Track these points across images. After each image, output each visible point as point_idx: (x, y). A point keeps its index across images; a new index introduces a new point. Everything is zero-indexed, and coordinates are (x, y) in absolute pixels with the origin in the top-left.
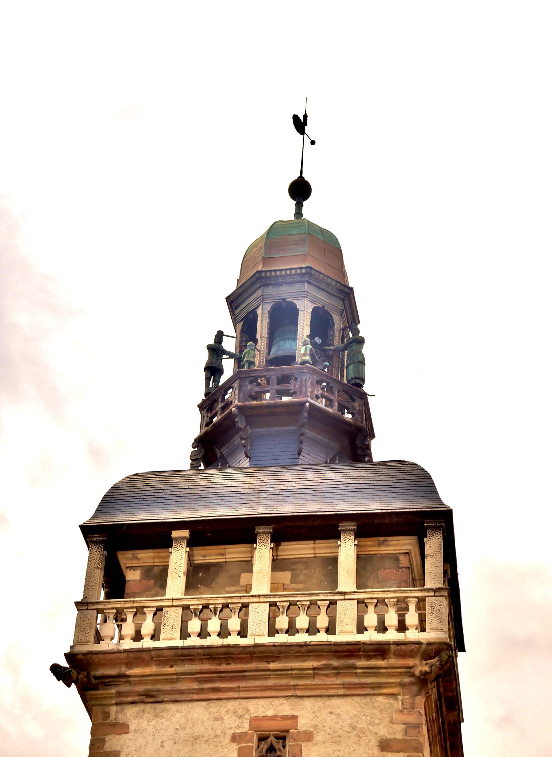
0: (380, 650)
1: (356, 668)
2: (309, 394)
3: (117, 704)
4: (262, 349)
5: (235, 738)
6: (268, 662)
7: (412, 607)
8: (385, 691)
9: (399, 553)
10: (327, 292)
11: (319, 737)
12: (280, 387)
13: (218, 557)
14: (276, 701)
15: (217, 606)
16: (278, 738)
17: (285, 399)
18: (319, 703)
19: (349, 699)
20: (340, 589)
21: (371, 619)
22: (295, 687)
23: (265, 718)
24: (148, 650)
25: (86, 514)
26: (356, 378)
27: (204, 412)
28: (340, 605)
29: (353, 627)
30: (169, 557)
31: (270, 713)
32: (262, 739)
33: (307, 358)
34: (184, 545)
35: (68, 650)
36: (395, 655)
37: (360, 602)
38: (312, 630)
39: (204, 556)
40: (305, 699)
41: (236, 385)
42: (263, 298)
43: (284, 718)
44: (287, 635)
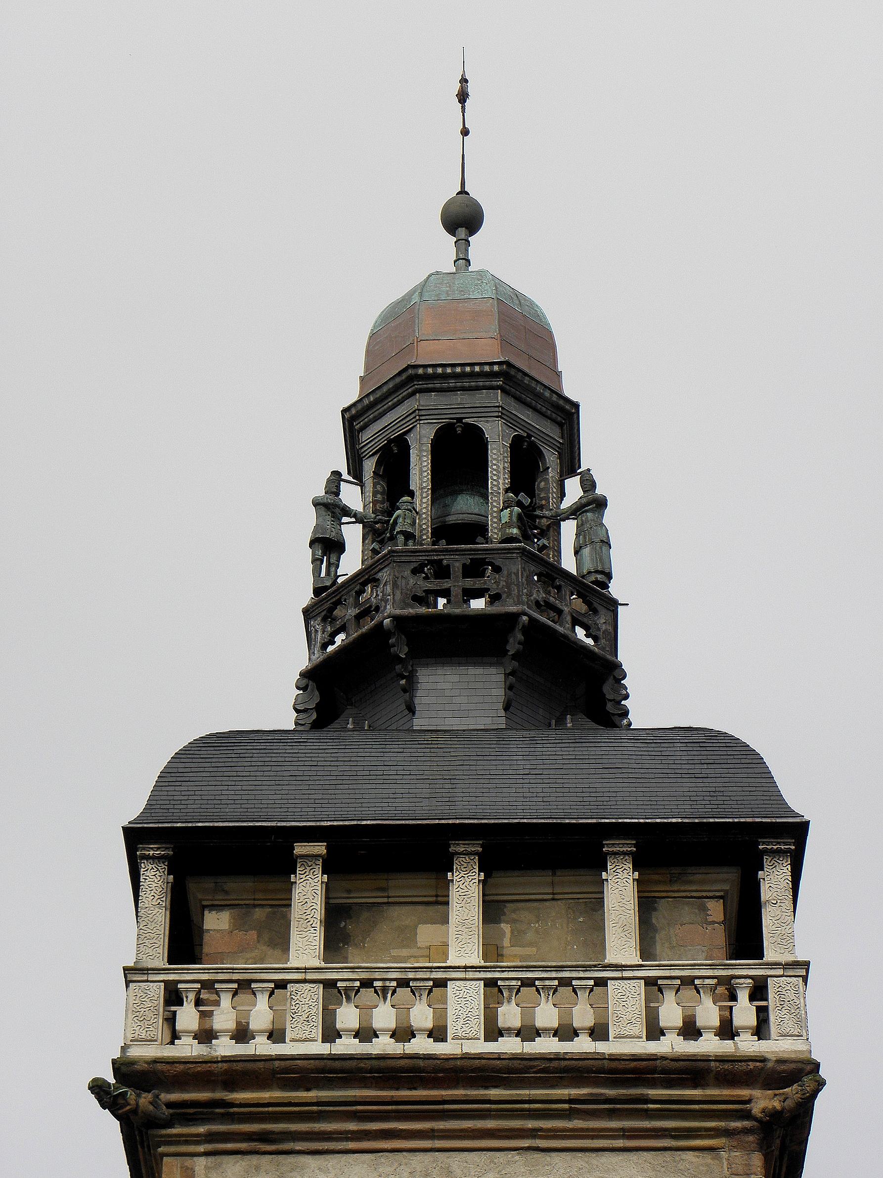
0: (692, 1071)
2: (525, 598)
4: (424, 511)
6: (486, 1088)
7: (743, 996)
9: (707, 897)
10: (535, 410)
12: (469, 583)
13: (374, 894)
15: (387, 983)
17: (478, 604)
18: (579, 1161)
19: (634, 1157)
20: (610, 959)
25: (132, 807)
26: (597, 572)
27: (316, 624)
29: (640, 1028)
30: (290, 891)
33: (515, 531)
34: (318, 870)
35: (117, 1055)
36: (717, 1079)
37: (650, 982)
38: (566, 1032)
39: (349, 891)
40: (553, 1154)
41: (384, 575)
42: (418, 415)
44: (519, 1039)
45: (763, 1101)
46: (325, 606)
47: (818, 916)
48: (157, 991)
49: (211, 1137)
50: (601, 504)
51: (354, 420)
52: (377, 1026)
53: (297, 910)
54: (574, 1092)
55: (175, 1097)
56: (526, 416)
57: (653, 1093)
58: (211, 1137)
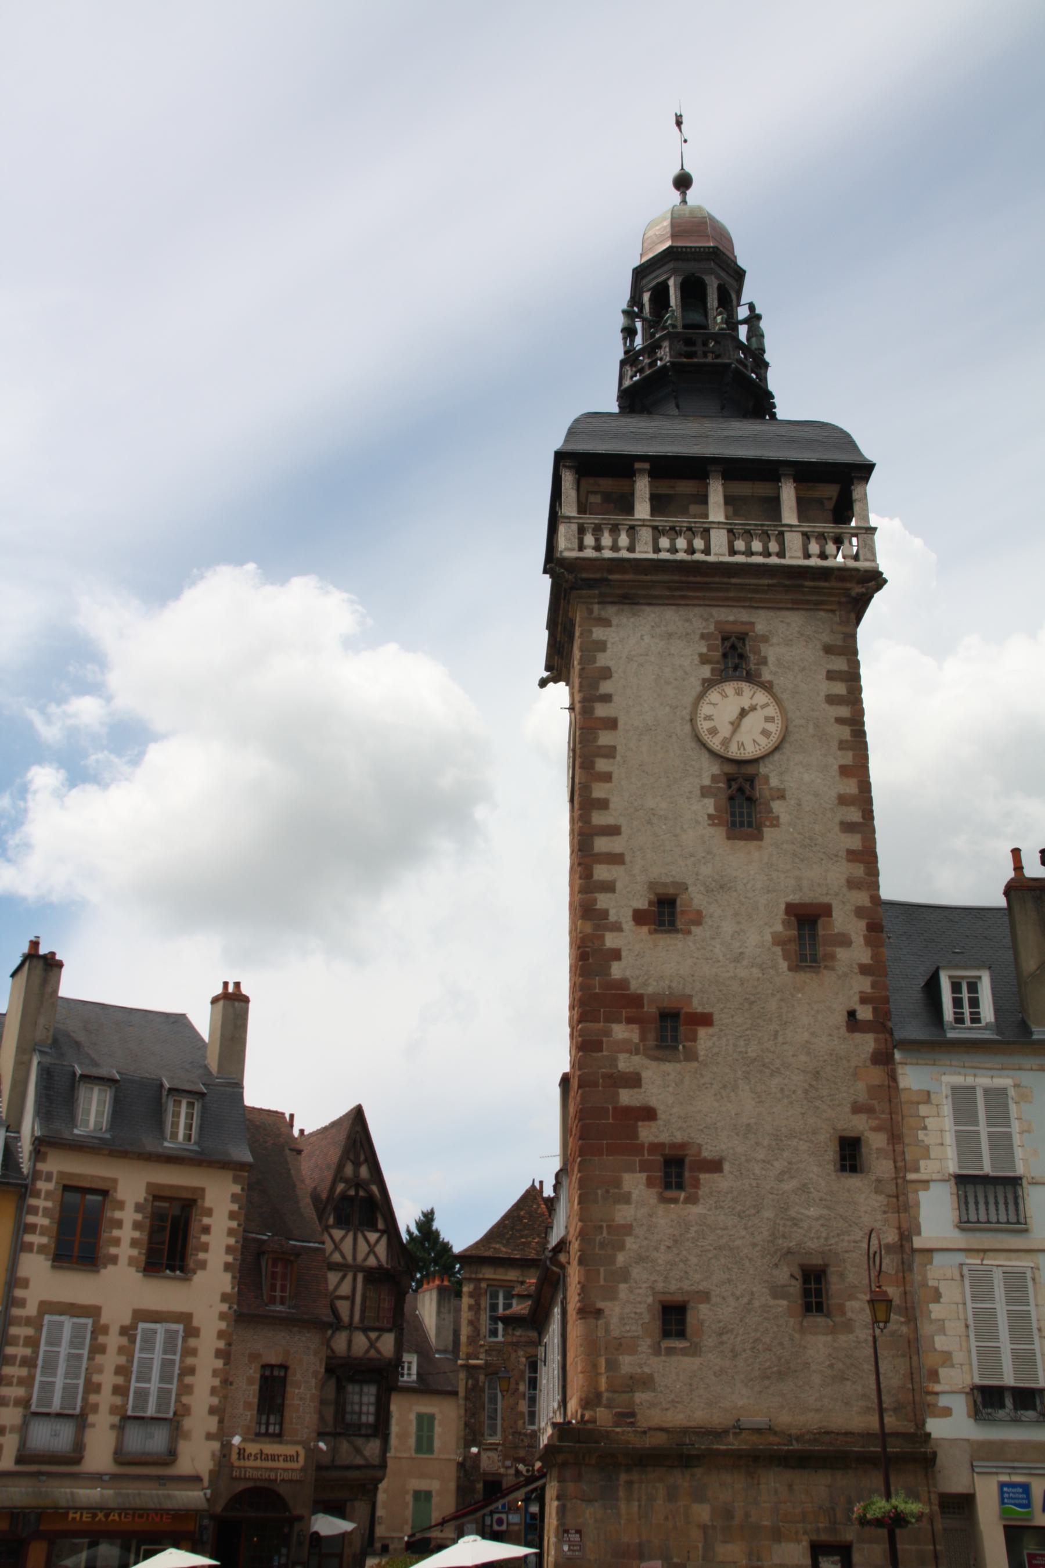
1: (803, 586)
3: (599, 603)
5: (703, 637)
8: (825, 607)
11: (774, 640)
14: (735, 610)
16: (738, 638)
18: (771, 613)
21: (814, 548)
23: (727, 622)
24: (629, 560)
28: (787, 535)
29: (800, 554)
31: (731, 618)
32: (724, 639)
33: (724, 326)
34: (646, 476)
38: (767, 554)
43: (743, 623)
46: (630, 359)
47: (881, 505)
48: (574, 527)
50: (759, 317)
51: (640, 274)
52: (678, 549)
53: (638, 494)
56: (722, 274)
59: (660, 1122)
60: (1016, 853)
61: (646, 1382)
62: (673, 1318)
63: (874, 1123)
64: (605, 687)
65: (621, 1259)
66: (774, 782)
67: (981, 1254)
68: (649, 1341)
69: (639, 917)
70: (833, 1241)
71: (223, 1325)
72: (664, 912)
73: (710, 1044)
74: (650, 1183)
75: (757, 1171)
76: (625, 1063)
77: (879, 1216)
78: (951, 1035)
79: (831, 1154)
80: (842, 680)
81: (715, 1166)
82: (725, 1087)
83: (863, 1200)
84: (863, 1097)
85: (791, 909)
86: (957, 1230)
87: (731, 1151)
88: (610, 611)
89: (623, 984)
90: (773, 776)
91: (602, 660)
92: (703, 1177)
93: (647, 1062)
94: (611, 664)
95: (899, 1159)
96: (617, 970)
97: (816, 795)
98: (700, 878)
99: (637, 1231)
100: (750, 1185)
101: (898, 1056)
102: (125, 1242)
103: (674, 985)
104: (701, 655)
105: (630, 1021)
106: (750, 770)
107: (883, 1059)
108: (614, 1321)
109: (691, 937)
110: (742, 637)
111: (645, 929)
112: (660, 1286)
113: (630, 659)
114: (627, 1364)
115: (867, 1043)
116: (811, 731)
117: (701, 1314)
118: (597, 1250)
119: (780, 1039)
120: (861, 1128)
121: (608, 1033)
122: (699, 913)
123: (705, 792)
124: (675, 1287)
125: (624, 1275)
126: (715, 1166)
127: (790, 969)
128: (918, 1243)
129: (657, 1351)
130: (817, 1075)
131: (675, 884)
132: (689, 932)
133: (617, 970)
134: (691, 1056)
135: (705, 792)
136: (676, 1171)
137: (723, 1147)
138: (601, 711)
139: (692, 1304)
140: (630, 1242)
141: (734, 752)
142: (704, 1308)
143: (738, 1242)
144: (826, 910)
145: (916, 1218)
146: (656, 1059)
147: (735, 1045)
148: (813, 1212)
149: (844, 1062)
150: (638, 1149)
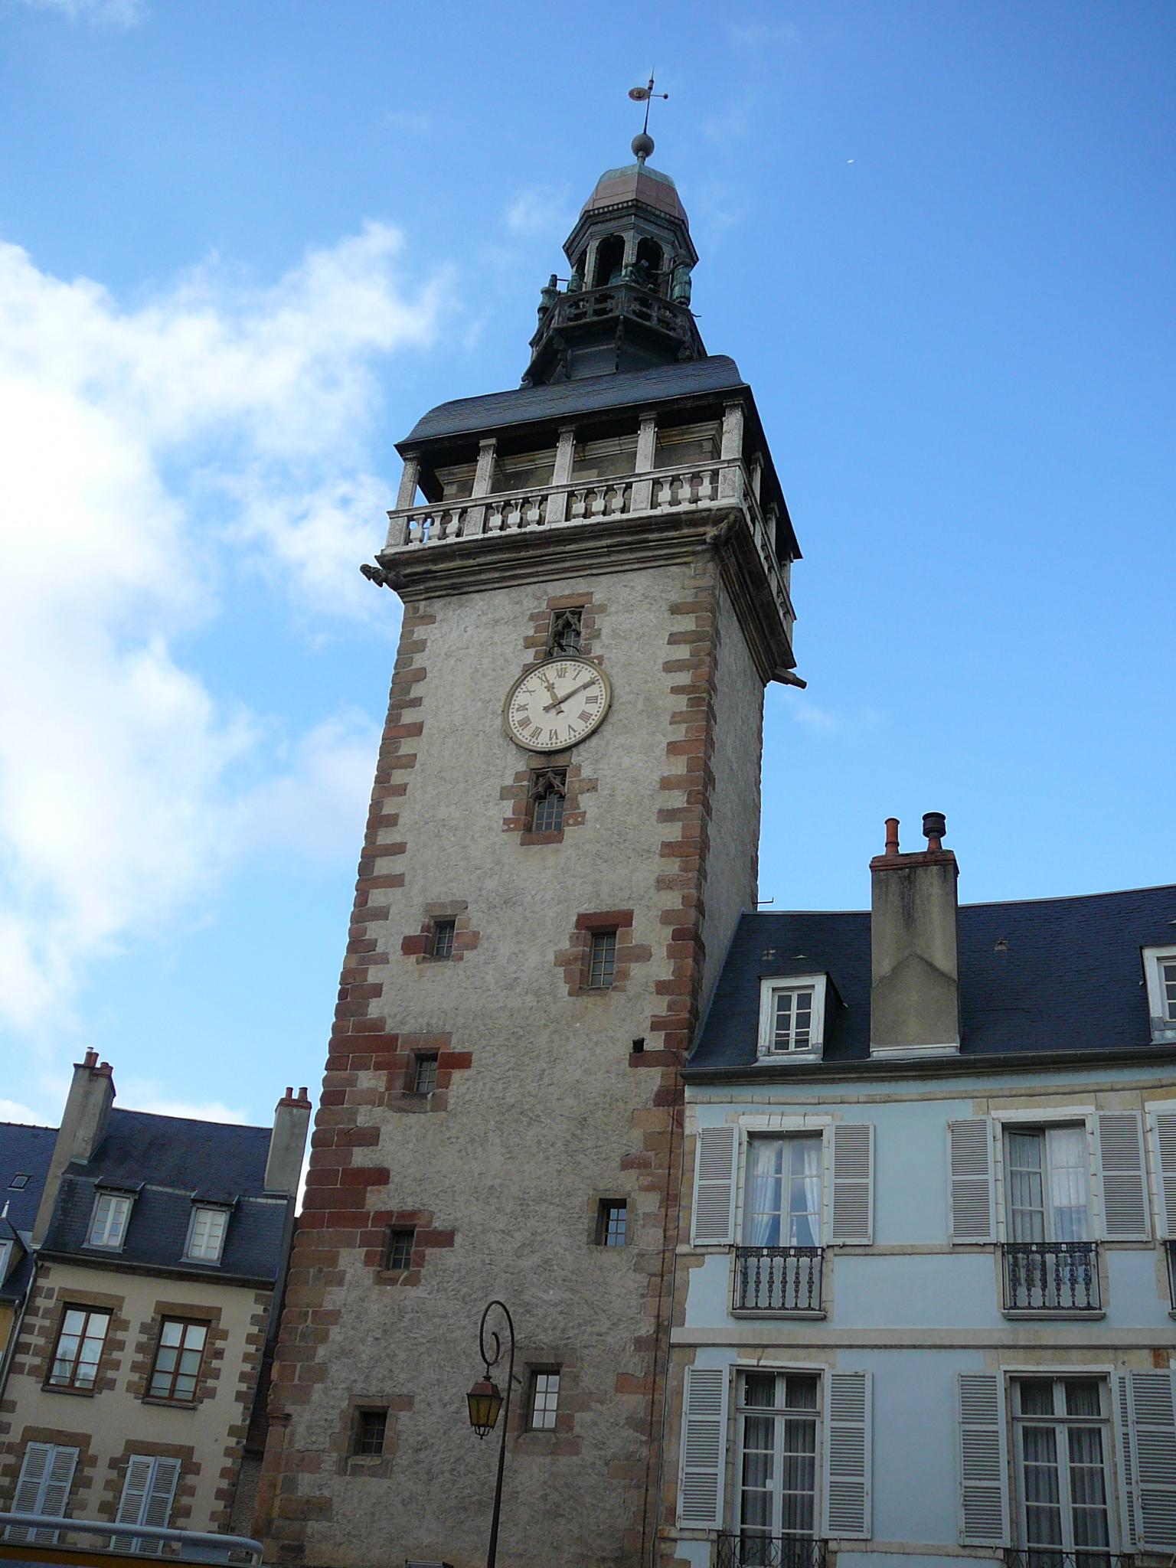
0: (672, 522)
5: (532, 618)
7: (706, 481)
19: (644, 572)
22: (590, 567)
29: (647, 504)
31: (567, 592)
32: (558, 616)
43: (583, 595)
45: (711, 532)
49: (427, 590)
54: (609, 542)
55: (409, 571)
57: (651, 536)
58: (427, 590)
59: (391, 1186)
60: (893, 824)
61: (321, 1508)
62: (369, 1426)
63: (646, 1181)
64: (417, 691)
65: (322, 1352)
66: (586, 773)
67: (760, 1350)
68: (335, 1455)
69: (409, 946)
70: (571, 1333)
71: (228, 1462)
72: (439, 937)
73: (463, 1089)
74: (368, 1261)
75: (493, 1245)
76: (365, 1118)
77: (635, 1302)
78: (764, 1061)
79: (587, 1221)
80: (686, 642)
81: (446, 1239)
82: (473, 1141)
83: (620, 1280)
84: (636, 1148)
85: (583, 921)
86: (731, 1319)
87: (466, 1220)
88: (438, 604)
89: (379, 1024)
90: (584, 763)
91: (419, 661)
92: (428, 1251)
93: (389, 1114)
94: (427, 664)
95: (671, 1226)
96: (375, 1009)
97: (634, 781)
98: (484, 893)
99: (347, 1318)
100: (483, 1261)
101: (688, 1093)
102: (126, 1366)
103: (433, 1021)
104: (526, 639)
105: (378, 1067)
106: (560, 761)
107: (670, 1099)
108: (301, 1429)
109: (462, 964)
110: (577, 612)
111: (413, 958)
112: (358, 1388)
113: (448, 655)
114: (307, 1484)
115: (653, 1078)
116: (640, 706)
117: (401, 1423)
118: (297, 1343)
119: (546, 1080)
120: (628, 1188)
121: (352, 1082)
122: (476, 934)
123: (505, 793)
124: (375, 1389)
125: (321, 1373)
126: (446, 1239)
127: (570, 994)
128: (677, 1336)
129: (342, 1472)
130: (583, 1122)
131: (453, 903)
132: (461, 958)
133: (375, 1009)
134: (440, 1105)
135: (505, 793)
136: (401, 1243)
137: (458, 1215)
138: (408, 717)
139: (390, 1411)
140: (335, 1333)
141: (543, 743)
142: (404, 1416)
143: (457, 1334)
144: (626, 918)
145: (682, 1304)
146: (400, 1110)
147: (492, 1089)
148: (552, 1295)
149: (620, 1104)
150: (360, 1219)
